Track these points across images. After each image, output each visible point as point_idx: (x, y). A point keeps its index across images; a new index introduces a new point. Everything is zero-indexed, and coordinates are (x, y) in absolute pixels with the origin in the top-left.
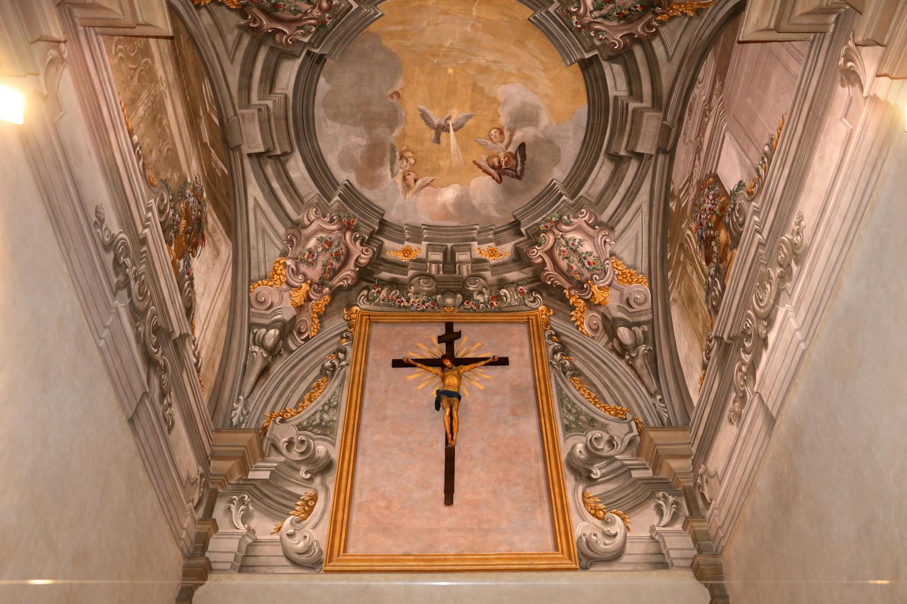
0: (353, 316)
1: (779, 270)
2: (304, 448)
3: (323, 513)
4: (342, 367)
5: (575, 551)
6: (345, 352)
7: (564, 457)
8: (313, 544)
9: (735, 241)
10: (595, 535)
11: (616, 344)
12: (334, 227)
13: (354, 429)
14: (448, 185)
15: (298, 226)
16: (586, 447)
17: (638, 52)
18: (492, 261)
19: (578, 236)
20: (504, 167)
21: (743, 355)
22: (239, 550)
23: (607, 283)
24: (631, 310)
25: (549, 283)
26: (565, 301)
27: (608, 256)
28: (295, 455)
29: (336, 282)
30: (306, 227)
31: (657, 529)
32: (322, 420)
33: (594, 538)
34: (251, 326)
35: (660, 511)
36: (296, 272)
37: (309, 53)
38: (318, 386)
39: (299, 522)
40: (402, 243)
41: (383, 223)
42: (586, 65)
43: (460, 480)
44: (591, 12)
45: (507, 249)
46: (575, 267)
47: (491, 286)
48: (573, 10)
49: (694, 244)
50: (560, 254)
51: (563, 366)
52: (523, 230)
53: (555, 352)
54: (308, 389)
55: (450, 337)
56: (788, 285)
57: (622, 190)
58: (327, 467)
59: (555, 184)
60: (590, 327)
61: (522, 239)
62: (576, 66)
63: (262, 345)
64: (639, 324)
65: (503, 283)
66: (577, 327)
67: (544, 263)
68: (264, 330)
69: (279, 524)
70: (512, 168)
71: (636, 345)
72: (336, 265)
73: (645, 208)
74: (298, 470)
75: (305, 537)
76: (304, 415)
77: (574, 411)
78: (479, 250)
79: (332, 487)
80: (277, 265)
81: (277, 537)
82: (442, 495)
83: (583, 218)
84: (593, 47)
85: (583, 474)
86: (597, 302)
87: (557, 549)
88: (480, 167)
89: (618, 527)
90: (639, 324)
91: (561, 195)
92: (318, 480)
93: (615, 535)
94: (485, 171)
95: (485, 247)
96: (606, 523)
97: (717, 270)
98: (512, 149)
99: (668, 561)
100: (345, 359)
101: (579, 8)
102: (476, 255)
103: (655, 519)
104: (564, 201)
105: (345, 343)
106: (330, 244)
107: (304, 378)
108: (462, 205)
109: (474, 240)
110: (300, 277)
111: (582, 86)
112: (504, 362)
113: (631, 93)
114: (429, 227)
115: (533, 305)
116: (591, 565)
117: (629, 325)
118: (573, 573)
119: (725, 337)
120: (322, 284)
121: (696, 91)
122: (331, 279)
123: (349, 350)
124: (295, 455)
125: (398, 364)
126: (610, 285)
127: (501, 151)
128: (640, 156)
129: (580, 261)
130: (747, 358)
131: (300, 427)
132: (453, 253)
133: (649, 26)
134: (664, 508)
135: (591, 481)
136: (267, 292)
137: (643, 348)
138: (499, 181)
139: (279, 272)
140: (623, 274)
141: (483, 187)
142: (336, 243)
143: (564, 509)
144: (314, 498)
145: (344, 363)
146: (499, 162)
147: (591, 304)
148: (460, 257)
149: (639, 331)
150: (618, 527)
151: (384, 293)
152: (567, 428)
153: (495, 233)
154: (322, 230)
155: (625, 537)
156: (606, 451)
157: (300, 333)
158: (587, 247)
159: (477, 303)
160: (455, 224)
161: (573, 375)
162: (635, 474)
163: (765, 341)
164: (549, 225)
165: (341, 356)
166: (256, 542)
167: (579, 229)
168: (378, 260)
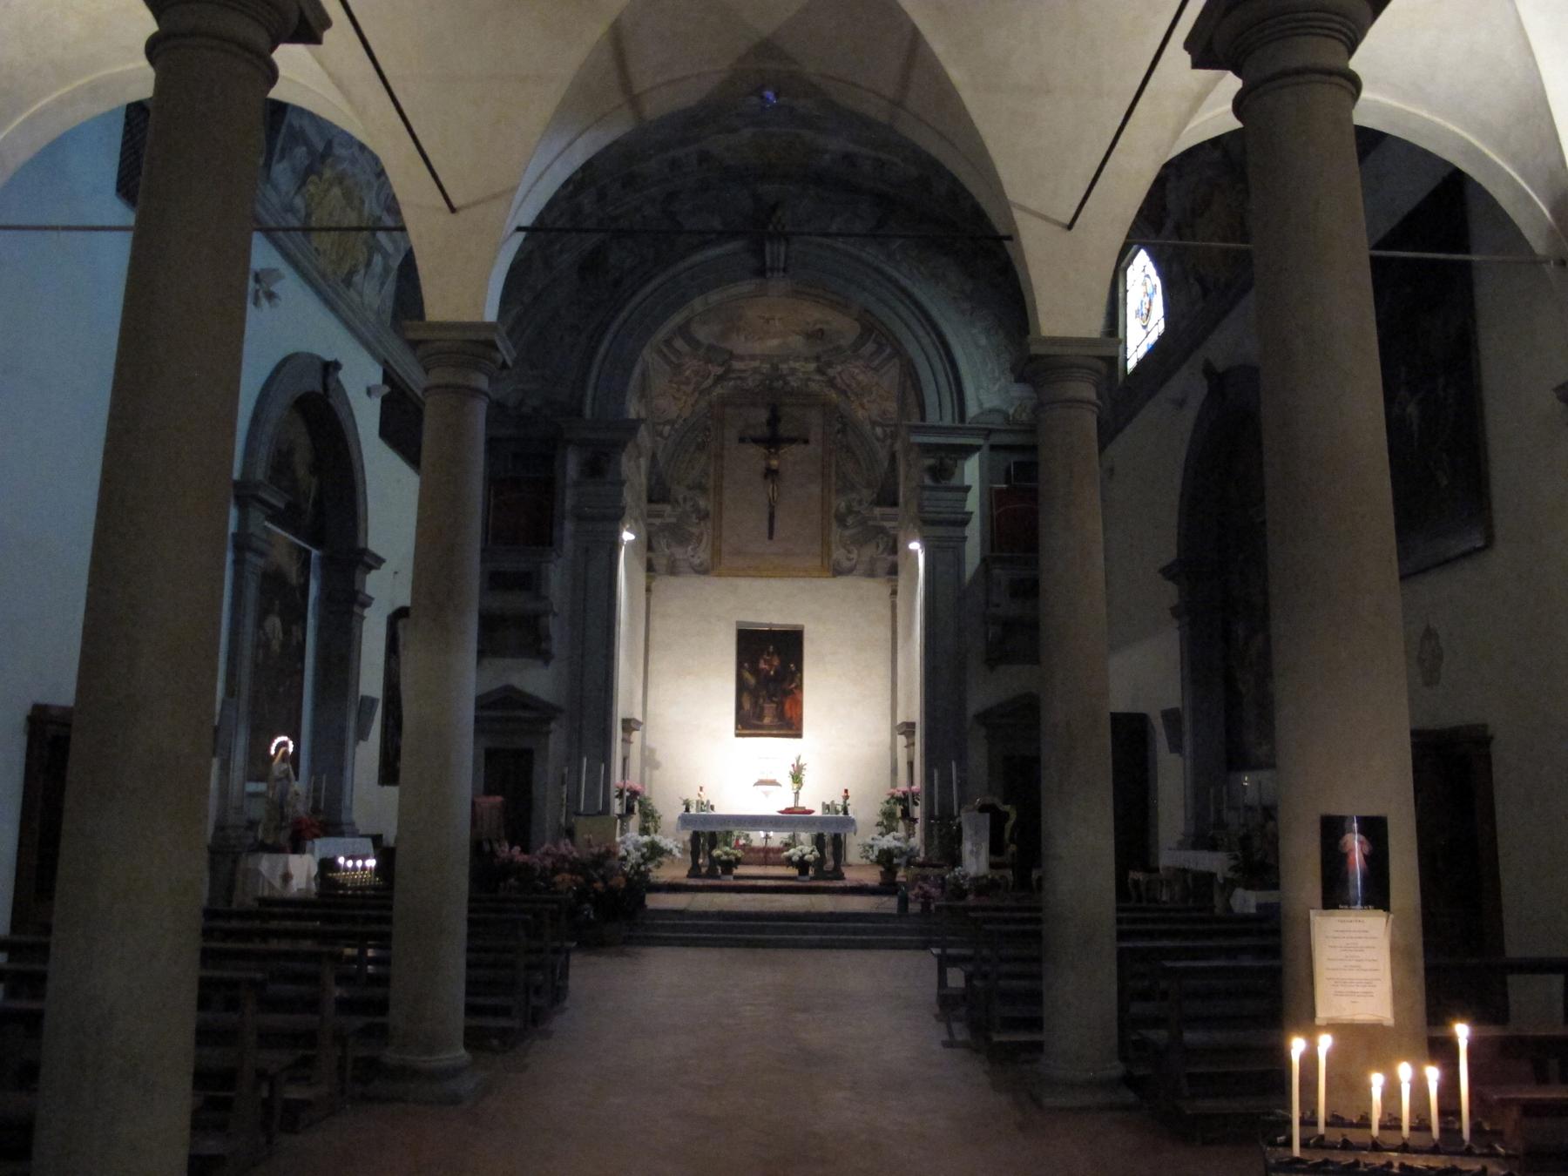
43: (777, 525)
45: (812, 366)
55: (774, 421)
58: (703, 516)
78: (792, 364)
83: (860, 363)
89: (854, 556)
112: (806, 442)
117: (882, 425)
124: (688, 507)
125: (742, 440)
135: (846, 527)
141: (797, 342)
152: (838, 491)
158: (861, 377)
162: (871, 523)
168: (729, 370)
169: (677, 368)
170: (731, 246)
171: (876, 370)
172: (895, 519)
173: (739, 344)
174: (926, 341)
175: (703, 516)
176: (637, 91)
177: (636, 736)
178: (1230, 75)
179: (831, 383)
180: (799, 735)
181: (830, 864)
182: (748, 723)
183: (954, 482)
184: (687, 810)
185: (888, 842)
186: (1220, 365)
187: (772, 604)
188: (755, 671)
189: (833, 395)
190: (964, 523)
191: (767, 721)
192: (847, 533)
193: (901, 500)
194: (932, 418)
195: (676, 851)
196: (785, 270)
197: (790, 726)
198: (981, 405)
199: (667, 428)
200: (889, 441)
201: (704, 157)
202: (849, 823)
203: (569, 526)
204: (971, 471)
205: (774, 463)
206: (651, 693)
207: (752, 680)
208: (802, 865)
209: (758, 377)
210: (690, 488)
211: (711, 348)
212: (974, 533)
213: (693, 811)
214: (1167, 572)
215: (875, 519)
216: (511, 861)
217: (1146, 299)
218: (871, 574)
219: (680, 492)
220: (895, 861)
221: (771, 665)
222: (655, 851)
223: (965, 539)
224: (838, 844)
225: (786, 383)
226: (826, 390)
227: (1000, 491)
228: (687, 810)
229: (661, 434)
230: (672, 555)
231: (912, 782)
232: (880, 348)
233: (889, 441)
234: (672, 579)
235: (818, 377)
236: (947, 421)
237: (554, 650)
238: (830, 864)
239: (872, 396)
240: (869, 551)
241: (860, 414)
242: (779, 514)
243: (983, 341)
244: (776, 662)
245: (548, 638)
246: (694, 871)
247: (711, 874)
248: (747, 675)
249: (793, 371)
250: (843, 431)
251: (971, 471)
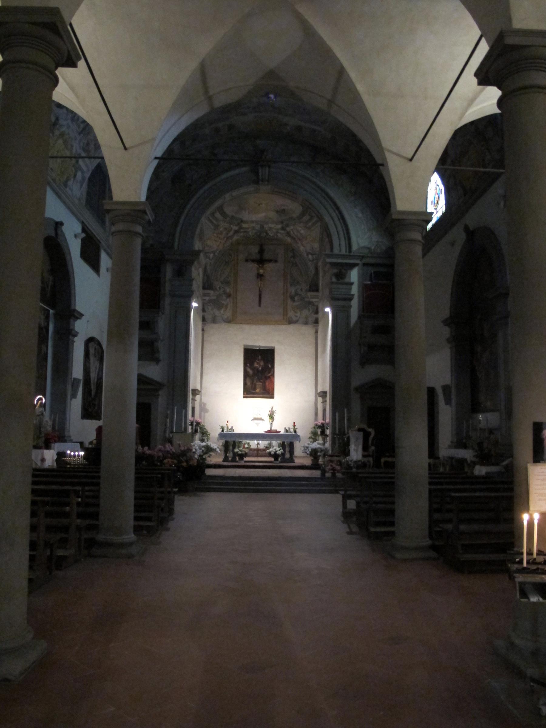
7: (289, 294)
35: (309, 310)
45: (279, 226)
64: (315, 254)
65: (278, 232)
78: (270, 225)
83: (302, 225)
85: (292, 298)
89: (298, 315)
96: (296, 312)
112: (276, 261)
117: (312, 255)
125: (247, 261)
135: (294, 301)
136: (209, 243)
141: (272, 215)
144: (228, 304)
149: (314, 256)
150: (298, 315)
152: (291, 285)
158: (302, 232)
162: (306, 300)
167: (300, 227)
168: (241, 228)
169: (217, 227)
170: (244, 169)
171: (309, 228)
172: (318, 298)
173: (245, 216)
174: (334, 215)
175: (229, 296)
176: (211, 93)
177: (198, 397)
178: (495, 88)
179: (288, 234)
180: (272, 397)
181: (287, 456)
182: (250, 391)
183: (346, 280)
184: (223, 431)
185: (315, 445)
186: (472, 226)
187: (260, 337)
188: (253, 369)
189: (289, 240)
190: (350, 299)
191: (258, 390)
193: (320, 288)
194: (336, 251)
195: (218, 450)
196: (268, 181)
197: (269, 393)
198: (358, 244)
200: (315, 261)
201: (231, 127)
202: (296, 436)
203: (167, 301)
204: (354, 275)
205: (261, 271)
206: (205, 378)
207: (250, 371)
208: (276, 456)
209: (254, 231)
210: (222, 283)
211: (233, 217)
212: (355, 304)
213: (225, 431)
214: (446, 322)
216: (144, 453)
217: (437, 196)
218: (306, 323)
219: (217, 285)
220: (319, 454)
221: (260, 365)
222: (209, 449)
223: (350, 307)
224: (291, 445)
225: (267, 234)
226: (286, 237)
227: (366, 285)
228: (223, 431)
229: (208, 258)
231: (324, 418)
232: (312, 217)
233: (315, 261)
234: (213, 325)
235: (282, 232)
236: (344, 251)
237: (161, 357)
238: (287, 456)
239: (308, 241)
240: (305, 312)
241: (302, 248)
242: (263, 296)
243: (360, 215)
244: (262, 363)
245: (158, 352)
246: (226, 459)
247: (234, 460)
248: (249, 370)
249: (270, 228)
250: (294, 256)
251: (354, 275)
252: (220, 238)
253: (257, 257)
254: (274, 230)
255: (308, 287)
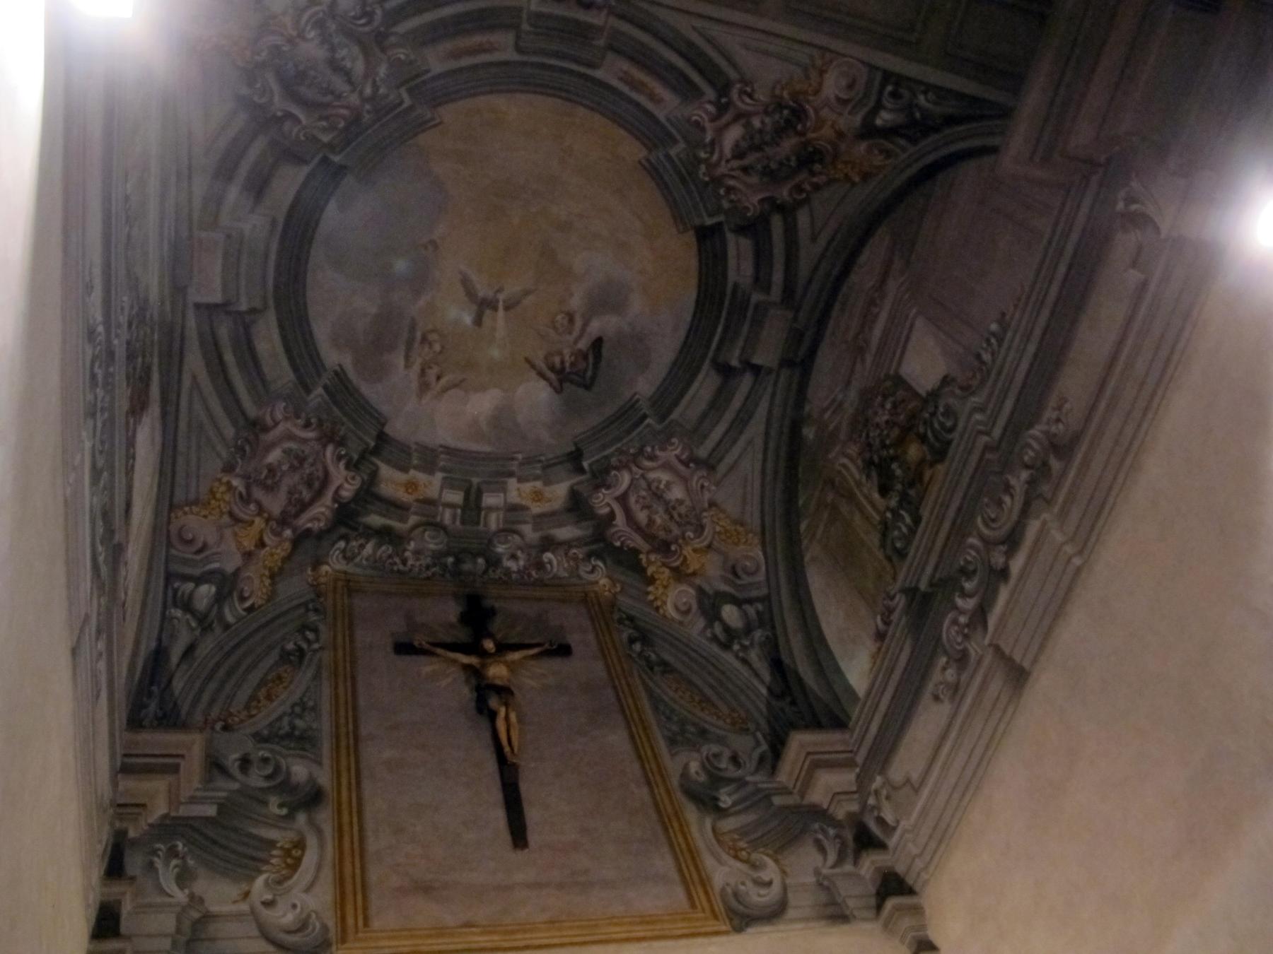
0: (323, 580)
1: (1025, 475)
2: (269, 770)
3: (319, 867)
4: (315, 651)
5: (719, 907)
6: (315, 630)
7: (675, 781)
8: (309, 916)
9: (940, 453)
10: (743, 884)
11: (718, 629)
12: (310, 434)
13: (350, 743)
14: (483, 388)
15: (257, 427)
16: (703, 767)
17: (777, 223)
18: (536, 509)
19: (665, 477)
20: (568, 370)
21: (959, 602)
22: (178, 930)
23: (706, 543)
24: (739, 582)
25: (618, 544)
26: (639, 569)
27: (706, 505)
28: (256, 779)
29: (304, 521)
30: (266, 429)
31: (825, 871)
32: (293, 727)
33: (742, 888)
34: (169, 577)
35: (822, 850)
36: (246, 499)
37: (325, 160)
38: (280, 678)
39: (279, 882)
40: (405, 469)
41: (382, 438)
42: (706, 236)
43: (533, 815)
44: (728, 161)
45: (559, 492)
46: (659, 521)
47: (530, 546)
48: (703, 155)
49: (854, 472)
50: (637, 502)
51: (647, 659)
52: (585, 464)
53: (632, 641)
54: (263, 683)
55: (477, 615)
56: (1045, 488)
57: (729, 416)
58: (313, 798)
59: (637, 401)
60: (677, 608)
61: (583, 478)
62: (690, 237)
63: (187, 606)
64: (750, 601)
65: (548, 544)
66: (657, 609)
67: (612, 516)
68: (190, 586)
69: (244, 887)
70: (579, 373)
71: (748, 630)
72: (306, 495)
73: (759, 442)
74: (265, 803)
75: (294, 906)
76: (261, 722)
77: (675, 719)
78: (516, 491)
79: (328, 829)
80: (217, 484)
81: (244, 907)
82: (506, 836)
83: (673, 452)
84: (720, 210)
85: (706, 801)
86: (690, 571)
87: (693, 906)
88: (533, 366)
90: (750, 601)
91: (645, 417)
92: (301, 818)
93: (770, 884)
94: (542, 375)
95: (528, 487)
96: (754, 866)
97: (904, 498)
98: (583, 345)
99: (848, 913)
100: (317, 640)
101: (712, 153)
102: (513, 497)
103: (819, 858)
104: (648, 425)
105: (313, 617)
106: (302, 460)
107: (253, 666)
108: (501, 420)
109: (511, 474)
110: (252, 507)
111: (694, 263)
112: (564, 650)
113: (757, 279)
114: (449, 451)
115: (592, 577)
116: (747, 925)
117: (738, 602)
118: (723, 939)
119: (923, 586)
120: (284, 521)
121: (854, 278)
122: (297, 515)
123: (322, 627)
125: (404, 648)
126: (709, 546)
127: (569, 346)
128: (757, 370)
129: (667, 511)
130: (969, 604)
131: (259, 738)
132: (479, 493)
133: (799, 188)
134: (826, 843)
135: (721, 813)
137: (758, 635)
138: (559, 390)
139: (218, 496)
140: (726, 531)
141: (535, 397)
142: (310, 460)
143: (693, 854)
144: (300, 845)
145: (316, 646)
146: (562, 362)
147: (679, 574)
148: (489, 500)
149: (751, 610)
150: (770, 871)
151: (369, 548)
152: (672, 742)
153: (545, 468)
154: (291, 437)
155: (785, 888)
156: (732, 772)
157: (243, 599)
158: (677, 493)
159: (508, 572)
160: (487, 448)
161: (664, 672)
162: (777, 800)
163: (1004, 573)
164: (624, 458)
165: (310, 635)
166: (208, 917)
167: (666, 466)
168: (368, 495)
171: (709, 465)
175: (313, 798)
179: (601, 544)
189: (600, 578)
192: (729, 824)
199: (206, 592)
200: (758, 635)
209: (432, 543)
210: (259, 738)
215: (784, 791)
218: (836, 915)
225: (493, 562)
229: (187, 606)
230: (196, 900)
235: (565, 533)
240: (807, 863)
241: (674, 599)
242: (527, 789)
252: (261, 510)
253: (463, 635)
254: (527, 529)
255: (764, 747)
